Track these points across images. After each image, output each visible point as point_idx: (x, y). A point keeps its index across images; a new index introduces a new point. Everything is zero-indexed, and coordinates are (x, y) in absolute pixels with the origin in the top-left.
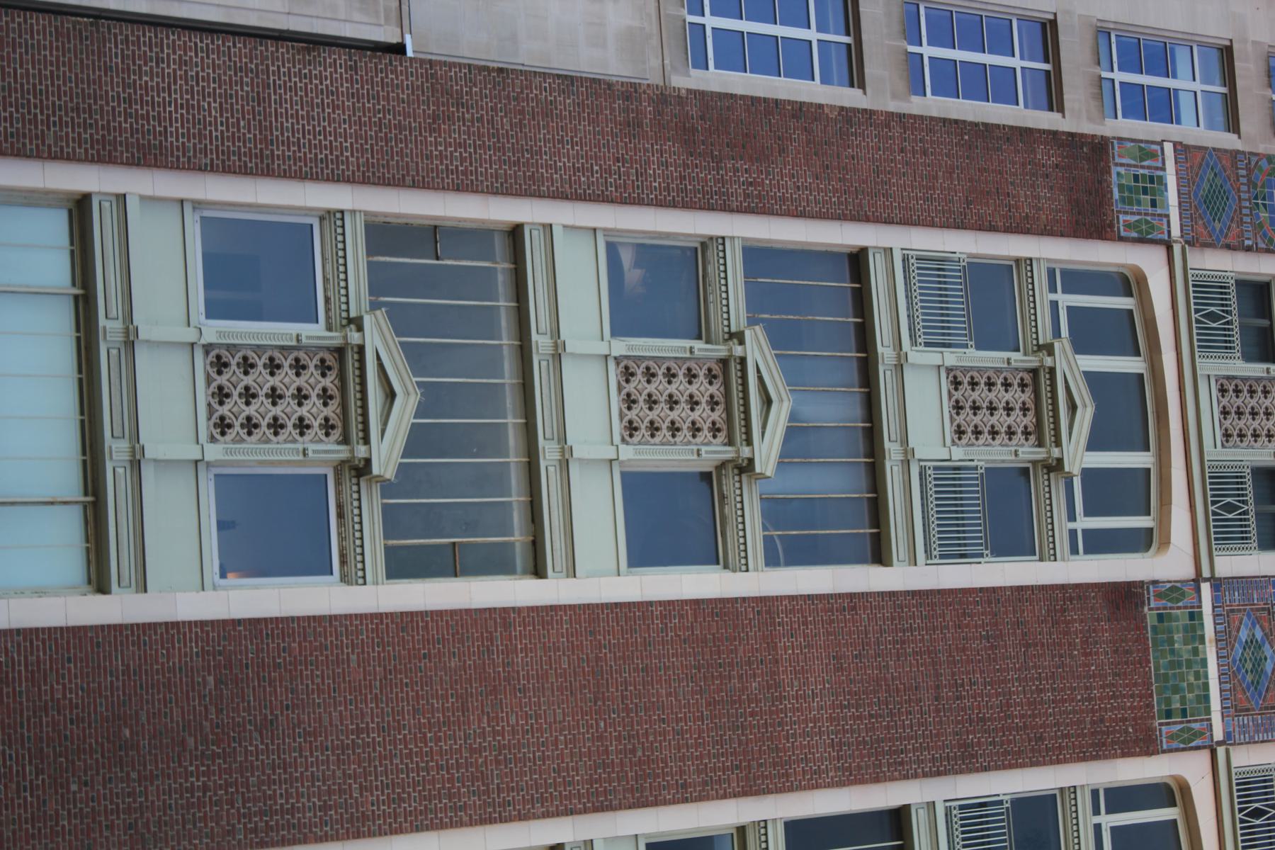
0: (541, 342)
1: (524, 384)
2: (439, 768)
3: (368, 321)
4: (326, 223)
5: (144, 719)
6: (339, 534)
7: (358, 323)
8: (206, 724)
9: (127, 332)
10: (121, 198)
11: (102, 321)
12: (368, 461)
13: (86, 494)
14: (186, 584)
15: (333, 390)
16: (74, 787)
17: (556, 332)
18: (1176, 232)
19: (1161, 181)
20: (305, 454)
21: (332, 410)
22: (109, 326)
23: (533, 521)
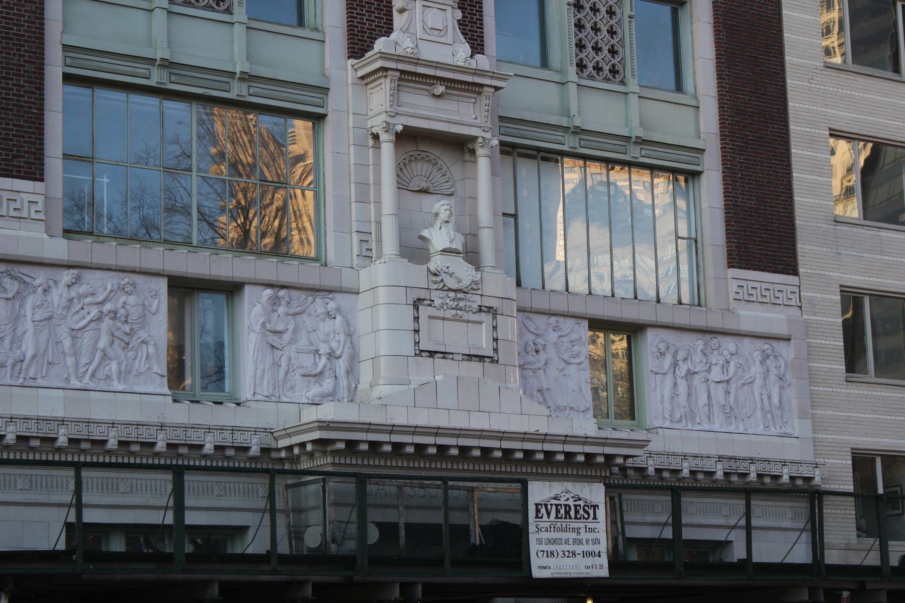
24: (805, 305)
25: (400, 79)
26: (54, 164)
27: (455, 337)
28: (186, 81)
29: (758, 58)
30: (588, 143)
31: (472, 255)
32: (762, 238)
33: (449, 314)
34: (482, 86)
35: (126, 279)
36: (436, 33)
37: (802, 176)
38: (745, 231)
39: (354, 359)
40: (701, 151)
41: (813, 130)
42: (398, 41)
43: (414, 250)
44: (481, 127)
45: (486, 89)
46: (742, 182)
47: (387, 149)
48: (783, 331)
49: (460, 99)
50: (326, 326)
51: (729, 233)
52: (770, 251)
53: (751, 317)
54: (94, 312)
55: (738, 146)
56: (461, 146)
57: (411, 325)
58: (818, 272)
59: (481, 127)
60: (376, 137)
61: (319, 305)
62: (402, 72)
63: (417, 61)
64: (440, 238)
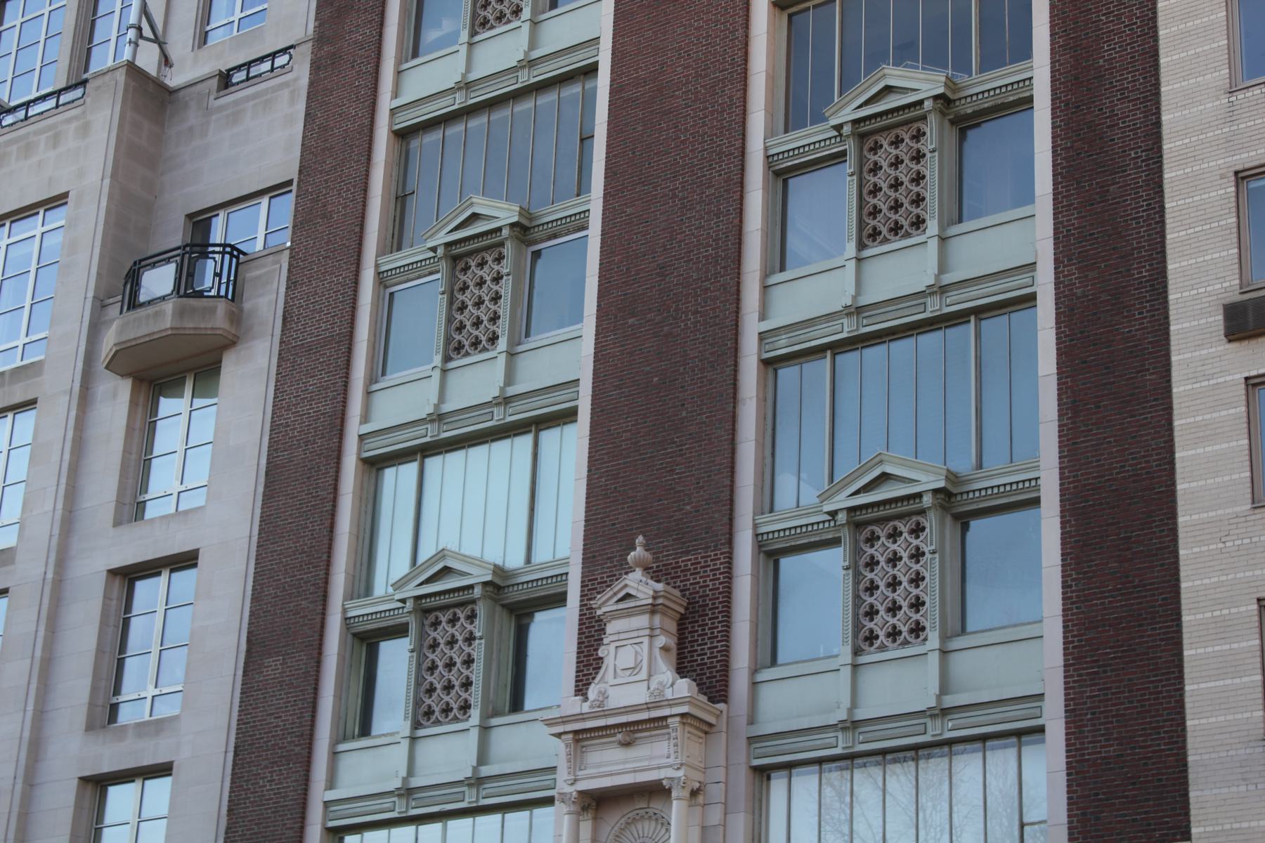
0: (459, 101)
1: (468, 114)
2: (704, 125)
3: (834, 121)
4: (388, 283)
5: (648, 368)
6: (566, 234)
7: (838, 128)
8: (658, 319)
9: (432, 421)
10: (362, 437)
11: (427, 439)
12: (936, 98)
13: (530, 432)
14: (567, 355)
15: (478, 259)
16: (684, 414)
17: (451, 90)
20: (934, 151)
22: (430, 434)
23: (572, 78)
25: (577, 741)
28: (427, 801)
29: (1130, 538)
30: (869, 735)
32: (1127, 797)
34: (665, 718)
36: (629, 672)
37: (1202, 686)
38: (1097, 794)
40: (553, 769)
41: (1225, 612)
44: (670, 766)
45: (669, 720)
46: (1094, 725)
49: (654, 739)
51: (1071, 802)
52: (1139, 814)
55: (1088, 674)
58: (1227, 827)
59: (670, 766)
62: (576, 732)
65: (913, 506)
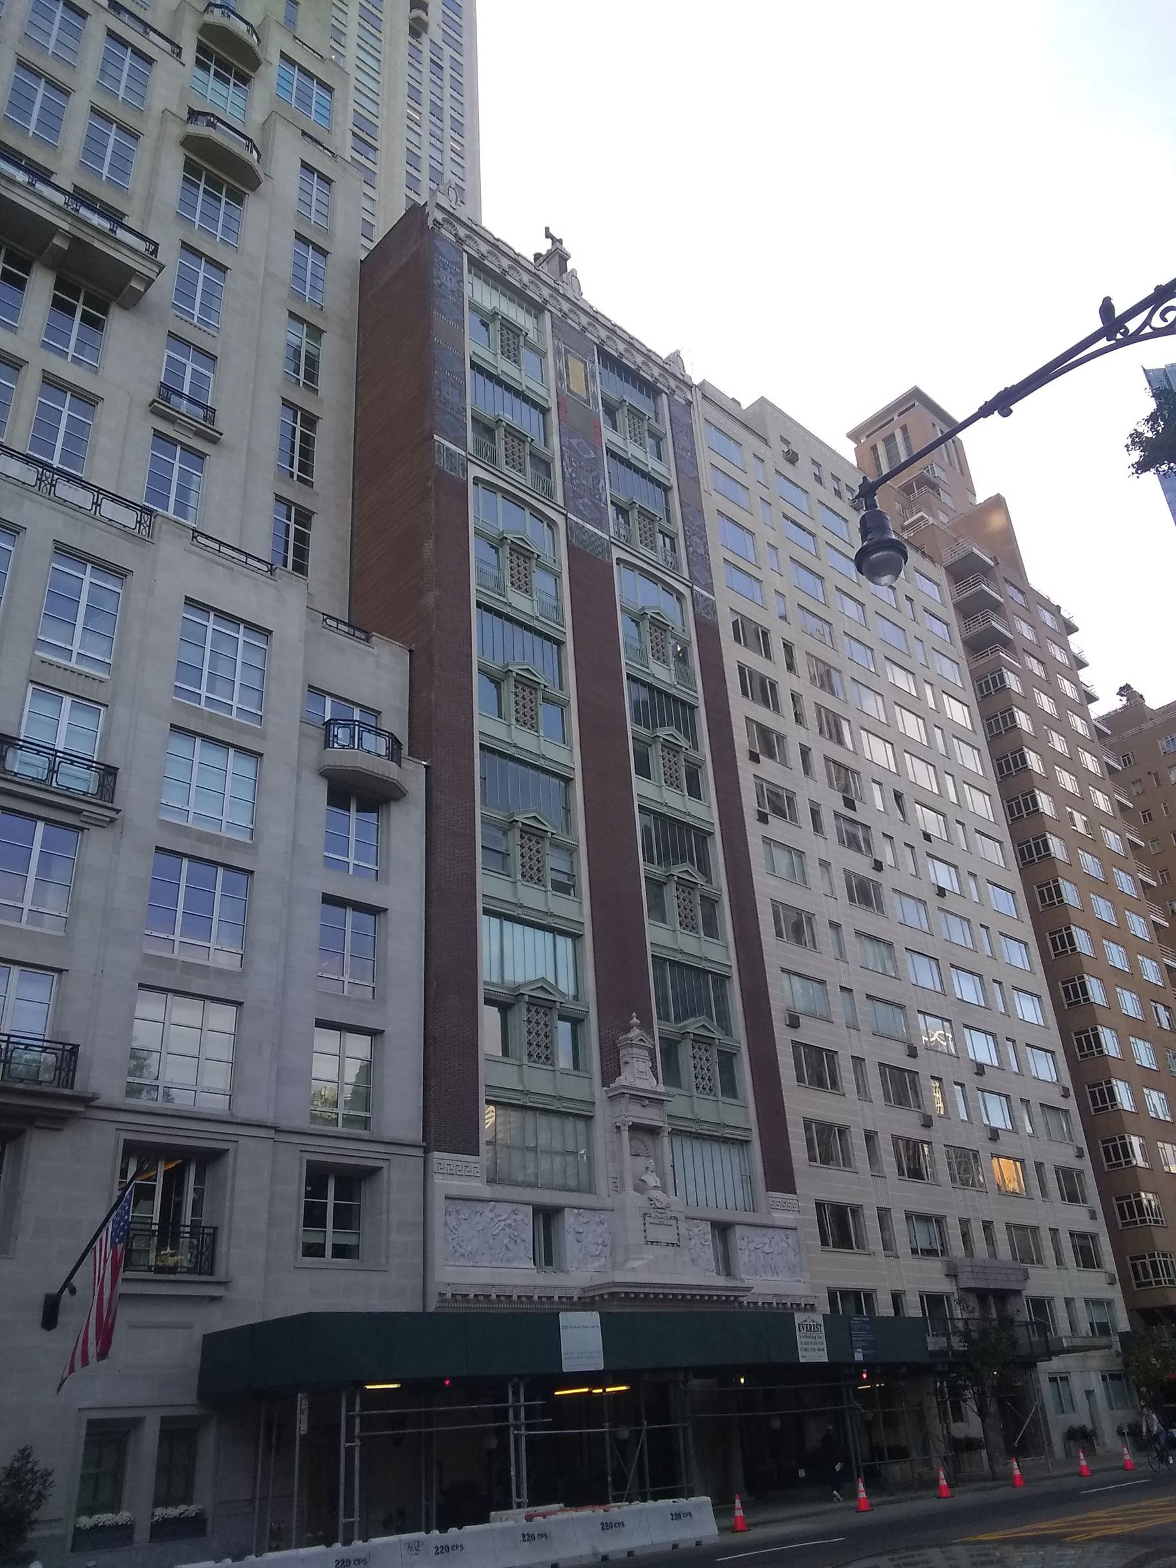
18: (463, 453)
19: (448, 449)
21: (534, 839)
22: (518, 912)
24: (796, 1213)
26: (483, 1147)
27: (664, 1234)
31: (664, 1189)
33: (657, 1221)
35: (515, 1206)
39: (613, 1246)
42: (625, 1079)
43: (640, 1187)
47: (626, 1134)
48: (794, 1225)
50: (601, 1229)
53: (780, 1217)
54: (502, 1223)
56: (653, 1131)
57: (642, 1227)
60: (618, 1128)
61: (596, 1217)
63: (638, 1089)
64: (652, 1180)
65: (709, 1041)
